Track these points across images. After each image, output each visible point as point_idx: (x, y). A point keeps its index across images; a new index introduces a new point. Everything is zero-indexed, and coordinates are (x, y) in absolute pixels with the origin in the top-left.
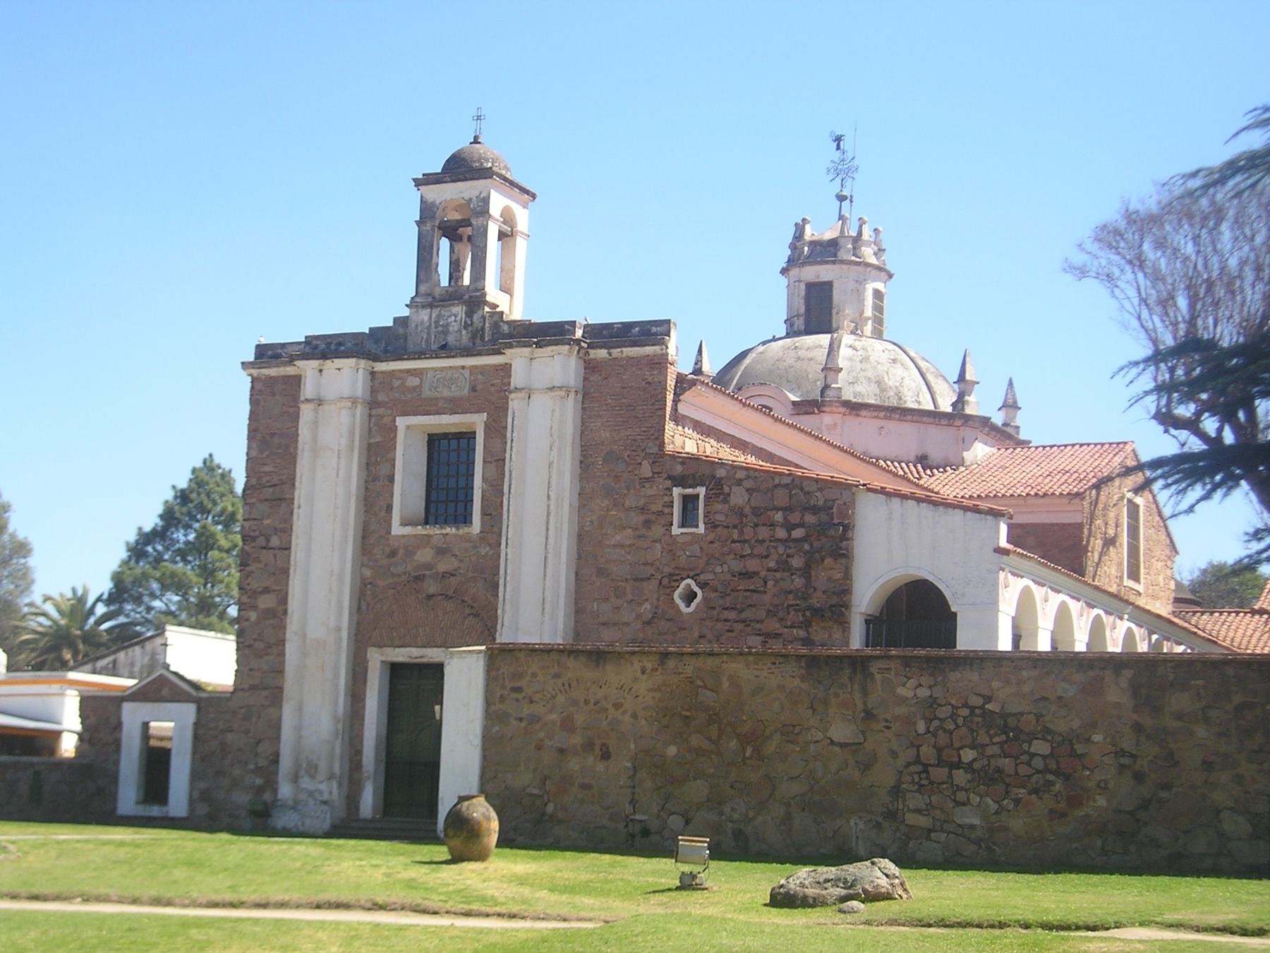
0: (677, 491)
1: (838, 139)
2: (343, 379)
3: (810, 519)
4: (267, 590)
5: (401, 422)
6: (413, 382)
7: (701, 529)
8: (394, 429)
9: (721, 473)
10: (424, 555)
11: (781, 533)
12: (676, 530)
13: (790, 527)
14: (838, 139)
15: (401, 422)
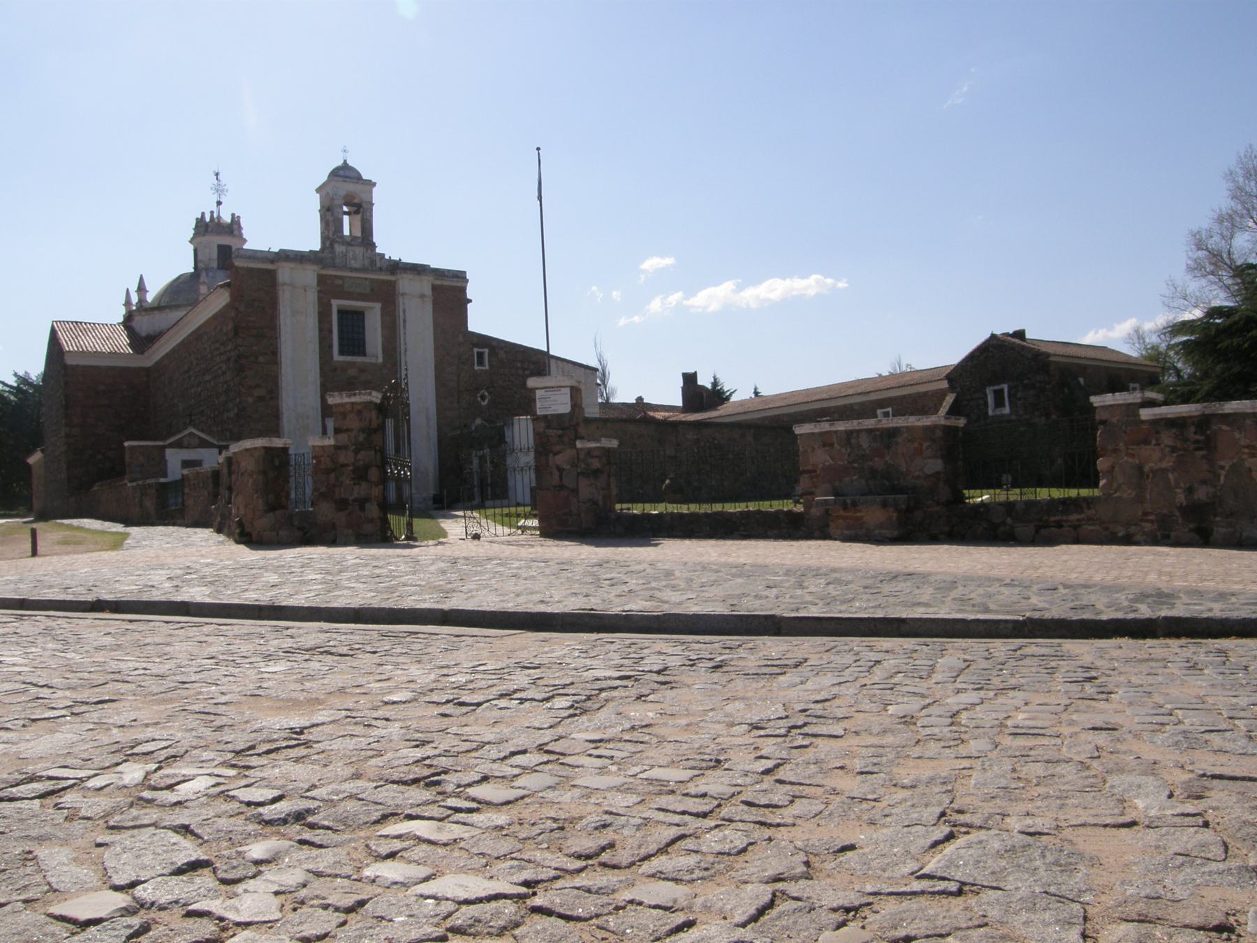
0: (476, 350)
1: (217, 174)
2: (309, 276)
3: (532, 367)
4: (257, 386)
5: (336, 304)
6: (339, 282)
7: (487, 367)
8: (331, 306)
9: (494, 343)
10: (352, 372)
11: (520, 372)
12: (476, 368)
13: (524, 370)
14: (217, 174)
15: (336, 304)
